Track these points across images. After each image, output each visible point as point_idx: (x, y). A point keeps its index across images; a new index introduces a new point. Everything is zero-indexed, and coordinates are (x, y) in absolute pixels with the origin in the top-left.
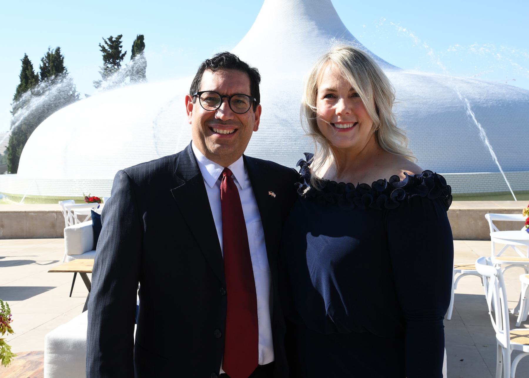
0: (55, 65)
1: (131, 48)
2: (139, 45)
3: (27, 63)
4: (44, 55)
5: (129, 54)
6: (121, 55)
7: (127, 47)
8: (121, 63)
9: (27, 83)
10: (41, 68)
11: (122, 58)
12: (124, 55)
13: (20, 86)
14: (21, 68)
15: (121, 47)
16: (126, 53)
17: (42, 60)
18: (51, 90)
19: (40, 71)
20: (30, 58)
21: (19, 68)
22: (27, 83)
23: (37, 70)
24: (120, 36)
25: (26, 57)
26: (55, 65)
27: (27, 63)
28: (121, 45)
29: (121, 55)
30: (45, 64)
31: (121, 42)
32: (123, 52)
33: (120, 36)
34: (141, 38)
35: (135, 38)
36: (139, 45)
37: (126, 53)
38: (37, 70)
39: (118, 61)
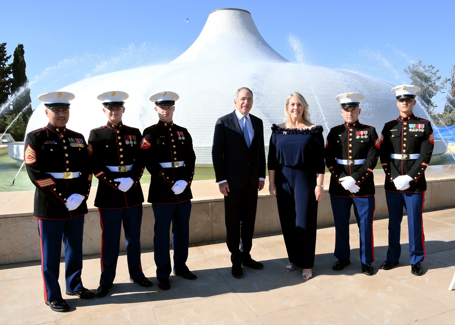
1: (13, 53)
2: (20, 51)
5: (13, 57)
6: (5, 57)
7: (10, 51)
8: (6, 63)
11: (6, 60)
12: (8, 58)
15: (6, 51)
16: (10, 56)
24: (5, 44)
28: (5, 50)
29: (5, 57)
31: (5, 48)
32: (7, 56)
33: (5, 44)
34: (21, 46)
35: (17, 46)
36: (20, 51)
37: (10, 56)
39: (3, 62)
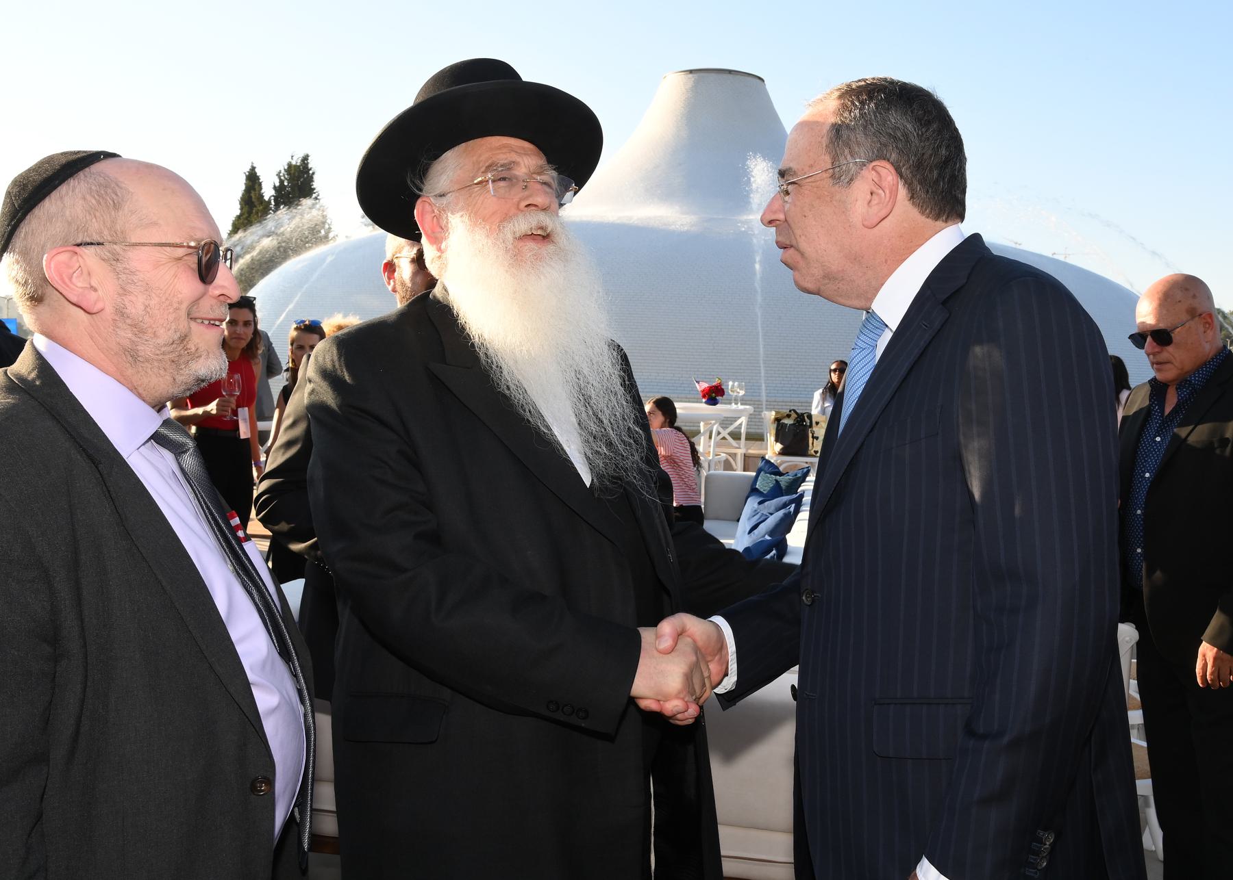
0: (299, 183)
3: (253, 179)
4: (282, 166)
9: (250, 213)
10: (275, 187)
13: (239, 217)
14: (243, 187)
17: (278, 175)
18: (286, 221)
19: (273, 192)
20: (259, 172)
21: (240, 186)
22: (250, 213)
23: (268, 192)
25: (253, 168)
26: (299, 183)
27: (253, 179)
30: (281, 182)
38: (268, 192)
